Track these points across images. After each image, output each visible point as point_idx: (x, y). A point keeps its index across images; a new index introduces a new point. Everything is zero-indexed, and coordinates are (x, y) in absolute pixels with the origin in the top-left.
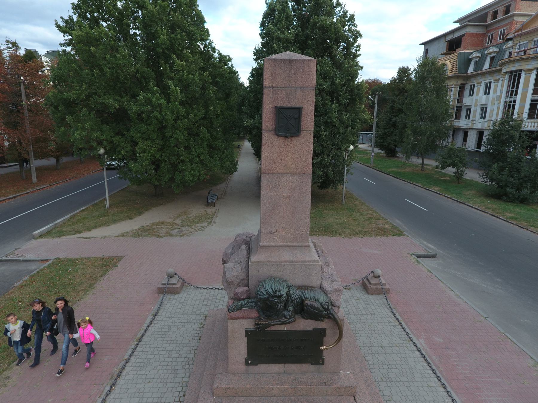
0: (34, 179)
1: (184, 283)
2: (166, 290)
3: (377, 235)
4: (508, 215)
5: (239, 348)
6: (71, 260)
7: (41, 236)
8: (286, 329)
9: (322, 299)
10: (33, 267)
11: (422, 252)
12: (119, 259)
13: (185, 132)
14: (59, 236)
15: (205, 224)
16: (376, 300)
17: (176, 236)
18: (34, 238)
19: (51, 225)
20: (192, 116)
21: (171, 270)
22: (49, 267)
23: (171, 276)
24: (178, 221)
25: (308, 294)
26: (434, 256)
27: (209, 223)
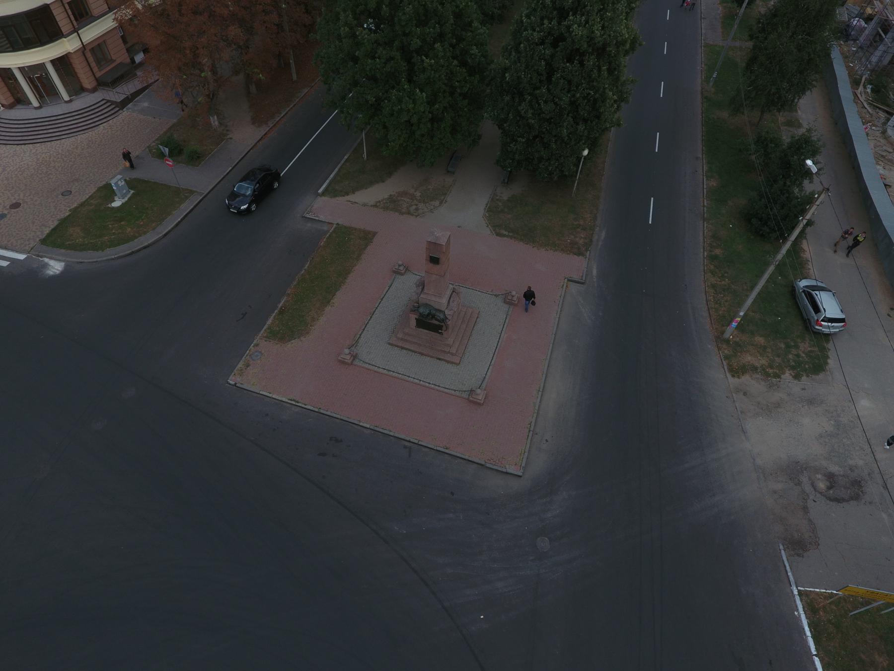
0: (295, 77)
1: (407, 269)
2: (397, 272)
3: (562, 250)
4: (718, 252)
5: (413, 323)
6: (346, 227)
7: (323, 194)
8: (430, 321)
9: (442, 316)
10: (326, 228)
11: (576, 277)
12: (375, 234)
13: (429, 125)
14: (335, 196)
15: (437, 203)
16: (507, 306)
17: (412, 215)
18: (318, 195)
19: (328, 181)
20: (437, 106)
21: (400, 263)
22: (334, 232)
23: (400, 266)
24: (418, 194)
25: (438, 314)
26: (583, 283)
27: (441, 203)
